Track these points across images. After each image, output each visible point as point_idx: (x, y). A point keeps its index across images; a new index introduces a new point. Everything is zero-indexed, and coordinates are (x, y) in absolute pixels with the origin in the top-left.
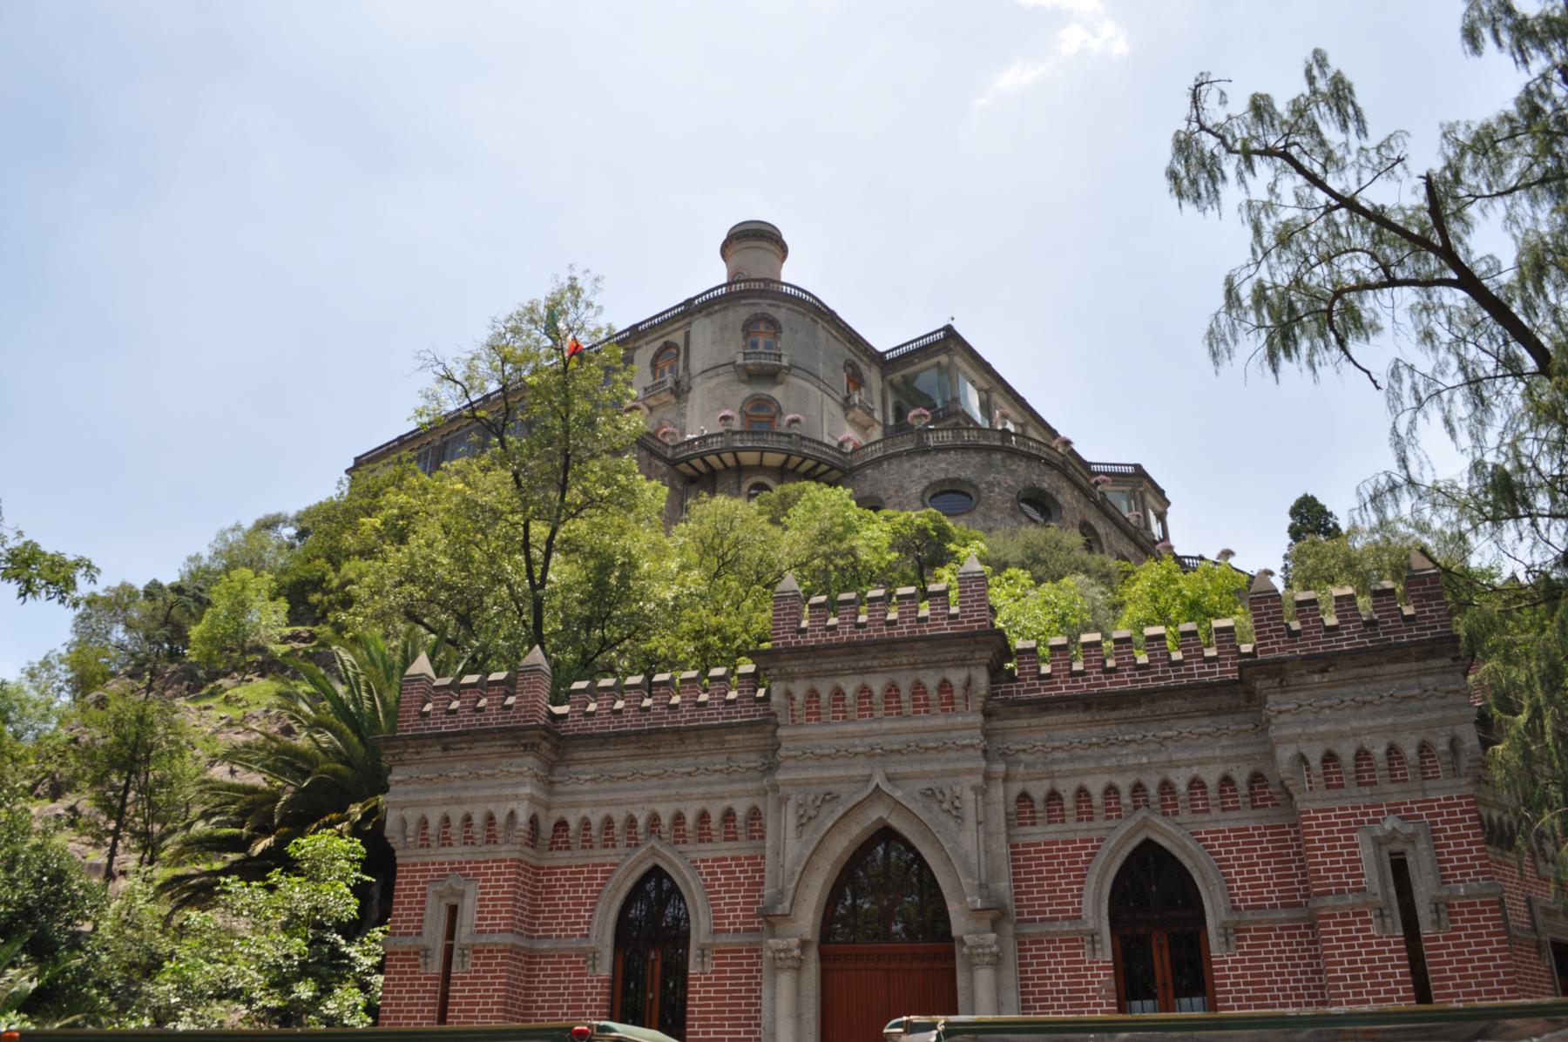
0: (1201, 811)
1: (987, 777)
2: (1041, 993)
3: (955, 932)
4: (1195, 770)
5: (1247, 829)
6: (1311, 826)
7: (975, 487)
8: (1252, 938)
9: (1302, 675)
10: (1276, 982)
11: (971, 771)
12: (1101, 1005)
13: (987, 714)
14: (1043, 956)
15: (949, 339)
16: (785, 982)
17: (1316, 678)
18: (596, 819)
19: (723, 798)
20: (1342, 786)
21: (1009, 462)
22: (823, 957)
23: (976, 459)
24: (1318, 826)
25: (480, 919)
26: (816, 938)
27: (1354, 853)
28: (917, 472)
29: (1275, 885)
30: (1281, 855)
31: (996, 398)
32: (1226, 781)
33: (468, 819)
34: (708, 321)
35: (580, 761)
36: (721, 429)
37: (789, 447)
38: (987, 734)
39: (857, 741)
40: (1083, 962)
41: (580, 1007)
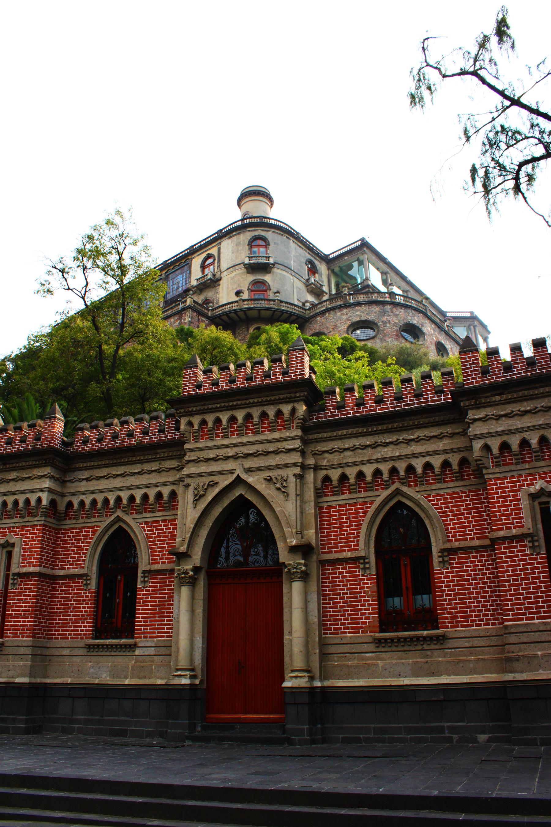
0: (431, 483)
1: (303, 467)
2: (333, 594)
3: (281, 561)
4: (428, 459)
5: (457, 493)
6: (492, 489)
7: (376, 324)
8: (459, 558)
9: (488, 397)
10: (472, 584)
11: (293, 465)
12: (368, 601)
13: (305, 429)
14: (335, 573)
15: (364, 245)
16: (185, 591)
17: (498, 398)
18: (88, 500)
19: (157, 486)
20: (512, 464)
21: (394, 310)
23: (376, 309)
24: (497, 489)
25: (23, 559)
26: (205, 566)
27: (518, 505)
28: (344, 317)
29: (474, 526)
30: (478, 508)
32: (446, 464)
33: (16, 503)
34: (229, 241)
35: (81, 469)
36: (237, 299)
37: (274, 307)
38: (305, 442)
39: (229, 450)
40: (359, 576)
41: (79, 608)
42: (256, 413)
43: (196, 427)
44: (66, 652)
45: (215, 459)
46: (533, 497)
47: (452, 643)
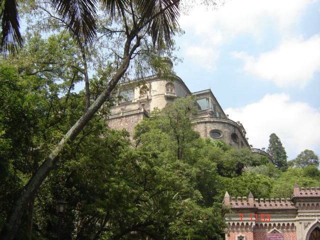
15: (210, 93)
31: (217, 107)
43: (302, 205)
45: (309, 216)
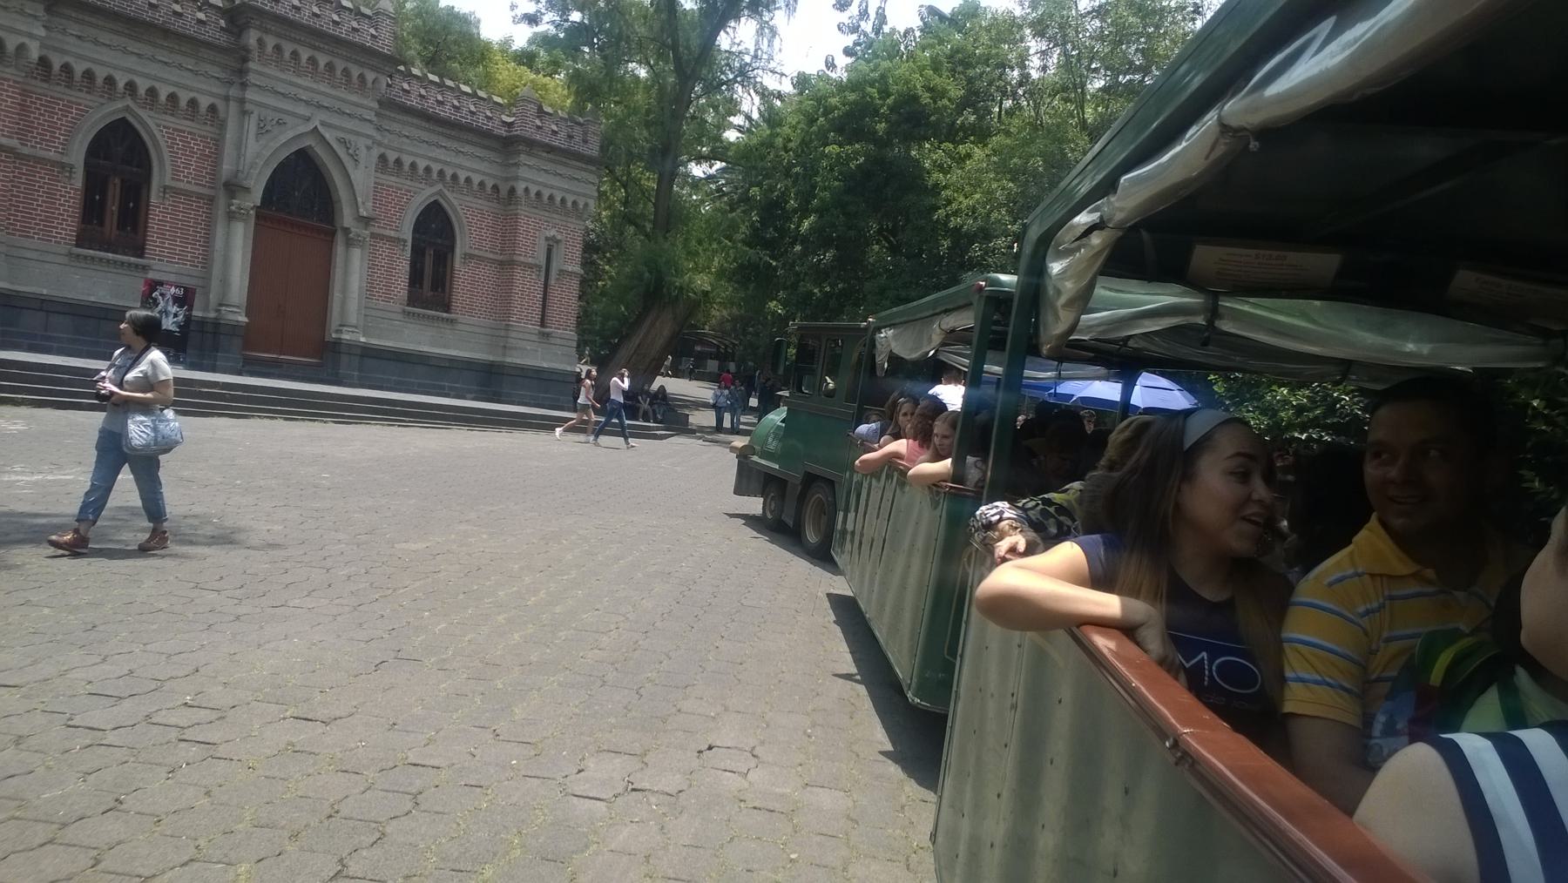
11: (368, 136)
22: (257, 217)
32: (482, 184)
35: (69, 18)
42: (340, 65)
43: (269, 49)
44: (28, 254)
46: (547, 239)
47: (460, 327)
